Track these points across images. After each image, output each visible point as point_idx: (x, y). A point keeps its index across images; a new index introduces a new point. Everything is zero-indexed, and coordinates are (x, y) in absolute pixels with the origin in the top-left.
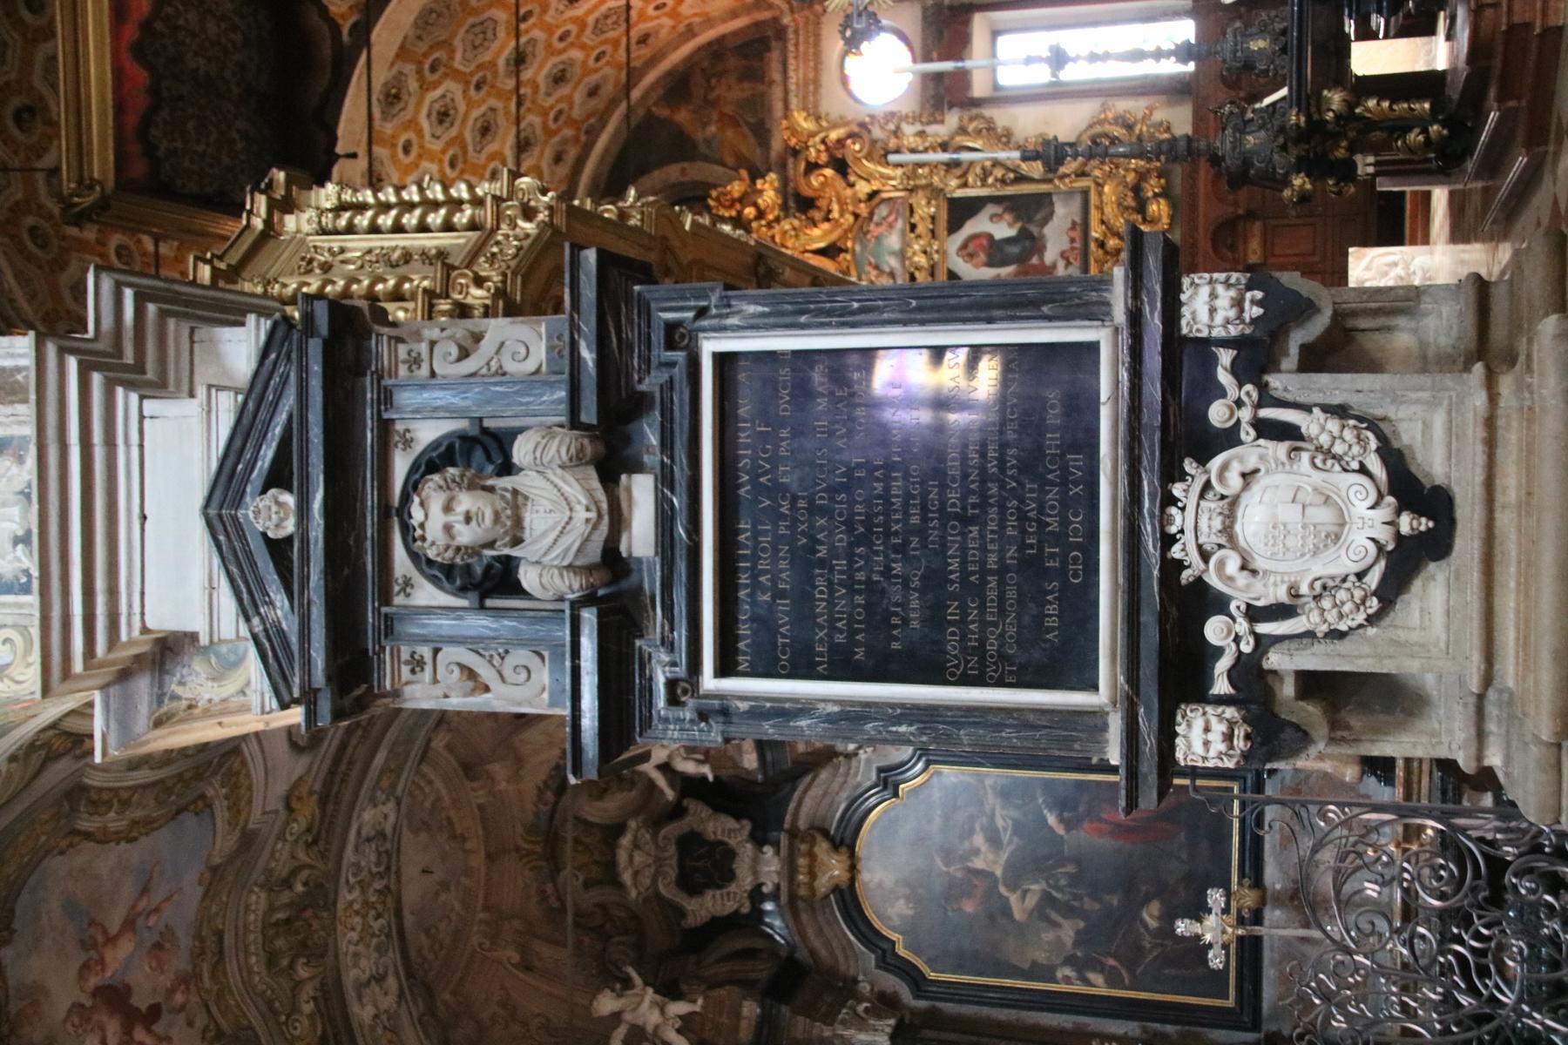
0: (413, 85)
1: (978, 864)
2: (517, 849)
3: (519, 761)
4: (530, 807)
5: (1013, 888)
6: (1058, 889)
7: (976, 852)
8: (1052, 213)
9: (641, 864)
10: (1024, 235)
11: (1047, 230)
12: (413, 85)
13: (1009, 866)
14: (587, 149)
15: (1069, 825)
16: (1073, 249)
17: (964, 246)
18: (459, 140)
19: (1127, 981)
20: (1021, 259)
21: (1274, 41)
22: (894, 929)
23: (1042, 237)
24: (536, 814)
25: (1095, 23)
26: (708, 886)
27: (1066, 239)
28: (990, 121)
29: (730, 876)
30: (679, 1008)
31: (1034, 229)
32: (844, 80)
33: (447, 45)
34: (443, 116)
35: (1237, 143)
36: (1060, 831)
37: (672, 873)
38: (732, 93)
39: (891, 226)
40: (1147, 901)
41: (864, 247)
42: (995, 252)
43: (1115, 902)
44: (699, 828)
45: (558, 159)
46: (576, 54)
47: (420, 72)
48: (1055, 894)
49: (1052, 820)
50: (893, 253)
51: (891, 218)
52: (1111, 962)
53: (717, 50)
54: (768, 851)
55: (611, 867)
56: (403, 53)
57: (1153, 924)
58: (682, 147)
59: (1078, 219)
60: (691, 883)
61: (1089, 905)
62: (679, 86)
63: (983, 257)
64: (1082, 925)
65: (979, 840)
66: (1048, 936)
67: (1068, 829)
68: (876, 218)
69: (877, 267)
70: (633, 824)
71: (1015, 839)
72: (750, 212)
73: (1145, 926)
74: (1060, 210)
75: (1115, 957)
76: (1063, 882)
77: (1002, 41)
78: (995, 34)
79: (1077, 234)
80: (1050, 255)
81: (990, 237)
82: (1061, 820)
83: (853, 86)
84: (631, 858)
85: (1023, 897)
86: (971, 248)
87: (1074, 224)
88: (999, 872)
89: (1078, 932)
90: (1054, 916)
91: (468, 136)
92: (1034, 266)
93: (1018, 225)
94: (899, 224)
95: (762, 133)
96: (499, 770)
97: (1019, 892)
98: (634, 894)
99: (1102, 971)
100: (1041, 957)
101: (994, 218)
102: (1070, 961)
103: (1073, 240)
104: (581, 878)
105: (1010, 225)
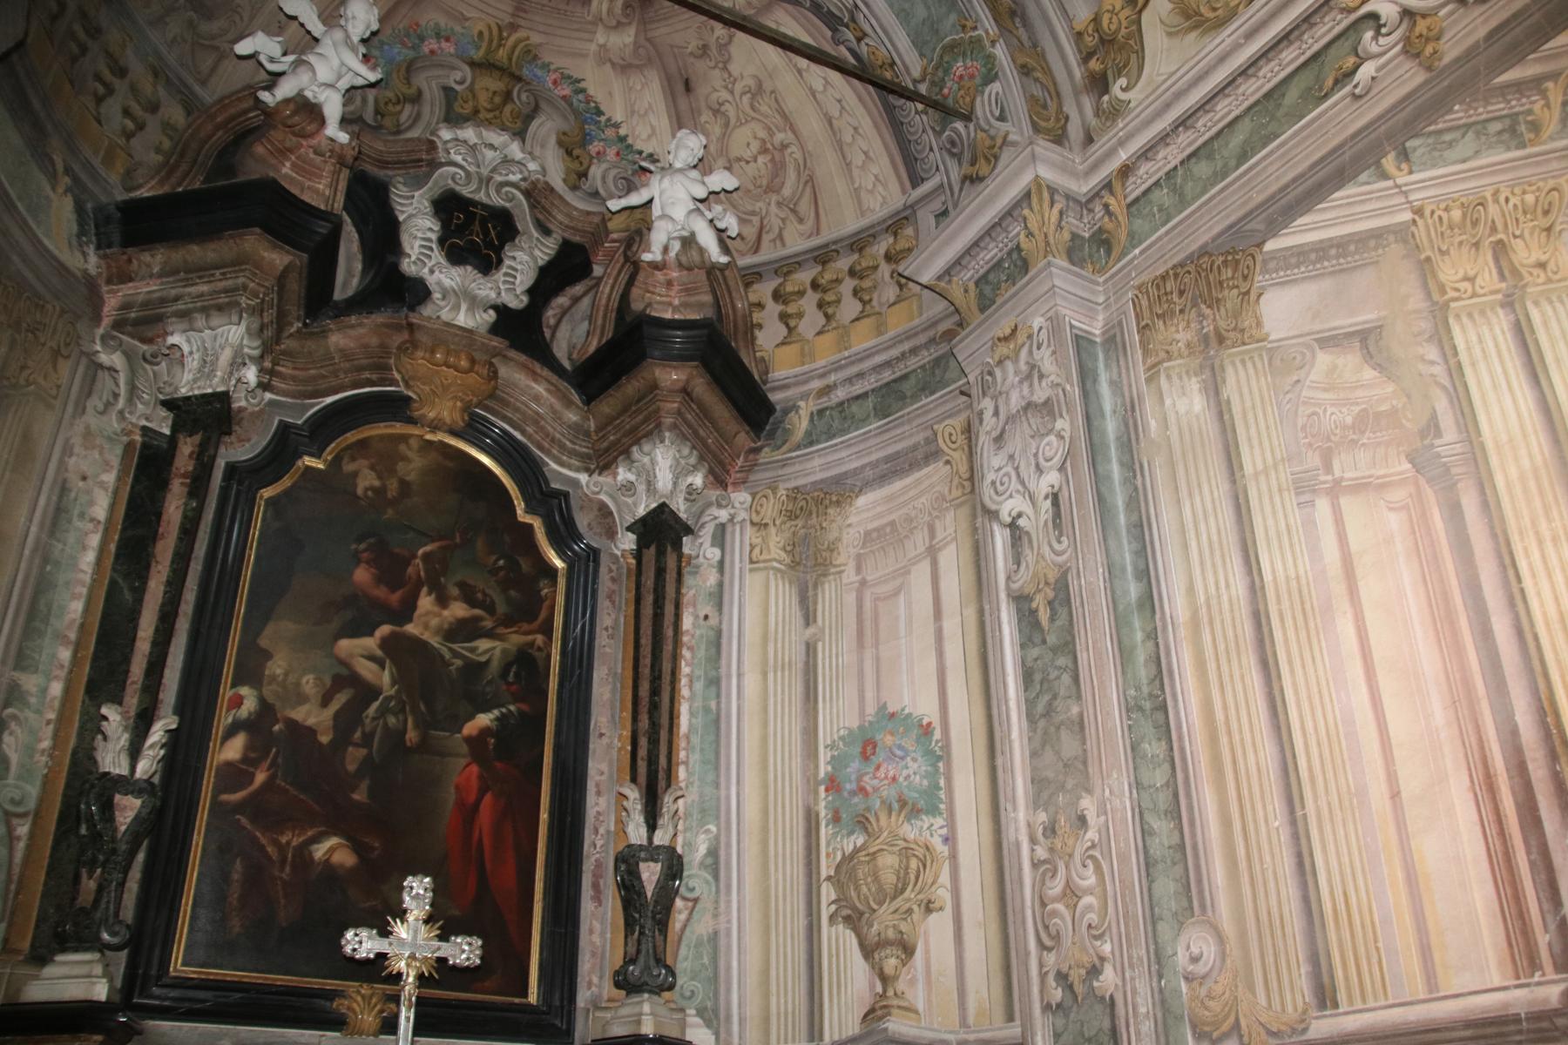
1: (426, 602)
2: (514, 27)
3: (624, 68)
4: (558, 62)
5: (385, 643)
6: (383, 712)
7: (443, 601)
9: (484, 159)
13: (419, 645)
15: (477, 743)
19: (224, 797)
22: (337, 461)
24: (546, 67)
26: (445, 225)
29: (455, 255)
30: (333, 107)
36: (470, 728)
37: (466, 192)
40: (358, 847)
43: (356, 796)
44: (521, 240)
48: (376, 705)
49: (484, 719)
52: (260, 777)
54: (491, 316)
55: (473, 117)
57: (320, 851)
60: (449, 207)
61: (354, 757)
64: (325, 739)
65: (459, 610)
66: (309, 683)
67: (469, 740)
70: (532, 166)
71: (459, 662)
73: (316, 839)
75: (268, 785)
76: (392, 720)
82: (485, 732)
84: (492, 147)
85: (372, 658)
88: (411, 629)
89: (312, 732)
90: (340, 700)
96: (624, 39)
97: (379, 653)
98: (446, 134)
99: (245, 759)
100: (277, 667)
102: (266, 709)
104: (457, 88)
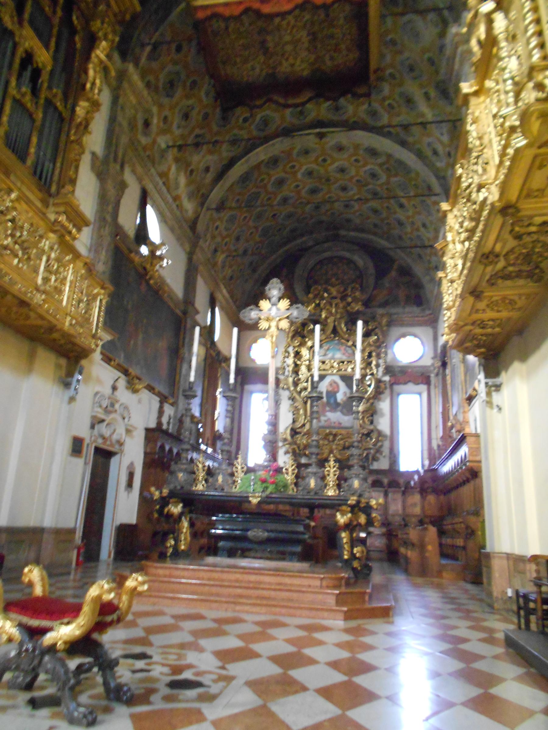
0: (380, 161)
10: (337, 405)
12: (380, 161)
14: (382, 237)
17: (335, 382)
18: (367, 184)
20: (328, 403)
21: (220, 486)
25: (422, 433)
31: (340, 408)
32: (404, 336)
33: (396, 175)
34: (374, 175)
35: (181, 470)
38: (401, 294)
39: (344, 354)
41: (336, 344)
42: (332, 394)
45: (375, 225)
46: (409, 229)
47: (384, 164)
50: (333, 355)
53: (419, 286)
56: (389, 156)
58: (381, 274)
62: (405, 272)
63: (330, 389)
68: (348, 348)
69: (328, 349)
72: (349, 299)
74: (346, 418)
77: (418, 396)
78: (420, 394)
81: (338, 391)
83: (402, 340)
86: (334, 385)
91: (370, 187)
94: (344, 358)
95: (385, 304)
101: (345, 393)
105: (342, 400)
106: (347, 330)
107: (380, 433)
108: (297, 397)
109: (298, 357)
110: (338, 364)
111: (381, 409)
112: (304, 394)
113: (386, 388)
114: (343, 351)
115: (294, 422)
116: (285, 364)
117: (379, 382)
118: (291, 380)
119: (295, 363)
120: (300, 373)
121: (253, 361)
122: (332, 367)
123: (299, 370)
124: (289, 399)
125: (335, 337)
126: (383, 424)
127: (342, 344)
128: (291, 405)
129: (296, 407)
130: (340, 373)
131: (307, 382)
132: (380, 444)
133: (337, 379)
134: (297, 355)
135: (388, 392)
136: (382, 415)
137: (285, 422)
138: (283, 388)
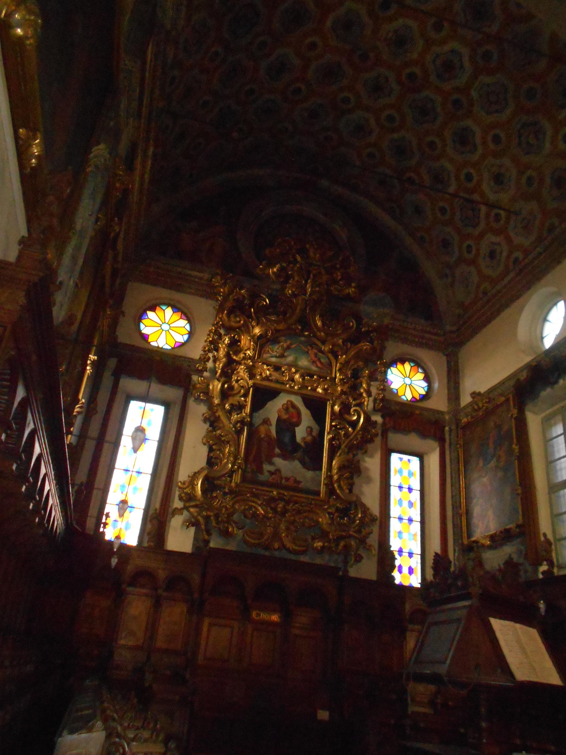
8: (308, 469)
10: (295, 446)
11: (297, 463)
16: (281, 478)
17: (294, 406)
20: (279, 442)
23: (293, 459)
27: (289, 475)
28: (371, 441)
31: (299, 454)
39: (314, 362)
51: (319, 364)
59: (301, 485)
63: (285, 417)
69: (288, 348)
74: (310, 474)
79: (290, 483)
80: (278, 461)
81: (298, 424)
86: (291, 410)
87: (299, 482)
92: (274, 448)
93: (303, 444)
94: (314, 368)
101: (310, 430)
103: (287, 479)
105: (304, 439)
106: (323, 324)
107: (365, 510)
108: (224, 419)
109: (235, 348)
110: (302, 376)
111: (367, 469)
112: (235, 417)
113: (377, 435)
114: (313, 356)
115: (210, 462)
116: (210, 355)
117: (367, 419)
118: (216, 386)
119: (228, 355)
120: (234, 378)
121: (145, 337)
122: (292, 380)
123: (233, 373)
124: (205, 420)
125: (302, 330)
126: (370, 497)
127: (312, 345)
128: (209, 432)
129: (219, 437)
130: (304, 392)
131: (245, 395)
132: (368, 530)
133: (298, 401)
134: (234, 345)
135: (378, 440)
136: (369, 480)
137: (193, 458)
138: (197, 399)
